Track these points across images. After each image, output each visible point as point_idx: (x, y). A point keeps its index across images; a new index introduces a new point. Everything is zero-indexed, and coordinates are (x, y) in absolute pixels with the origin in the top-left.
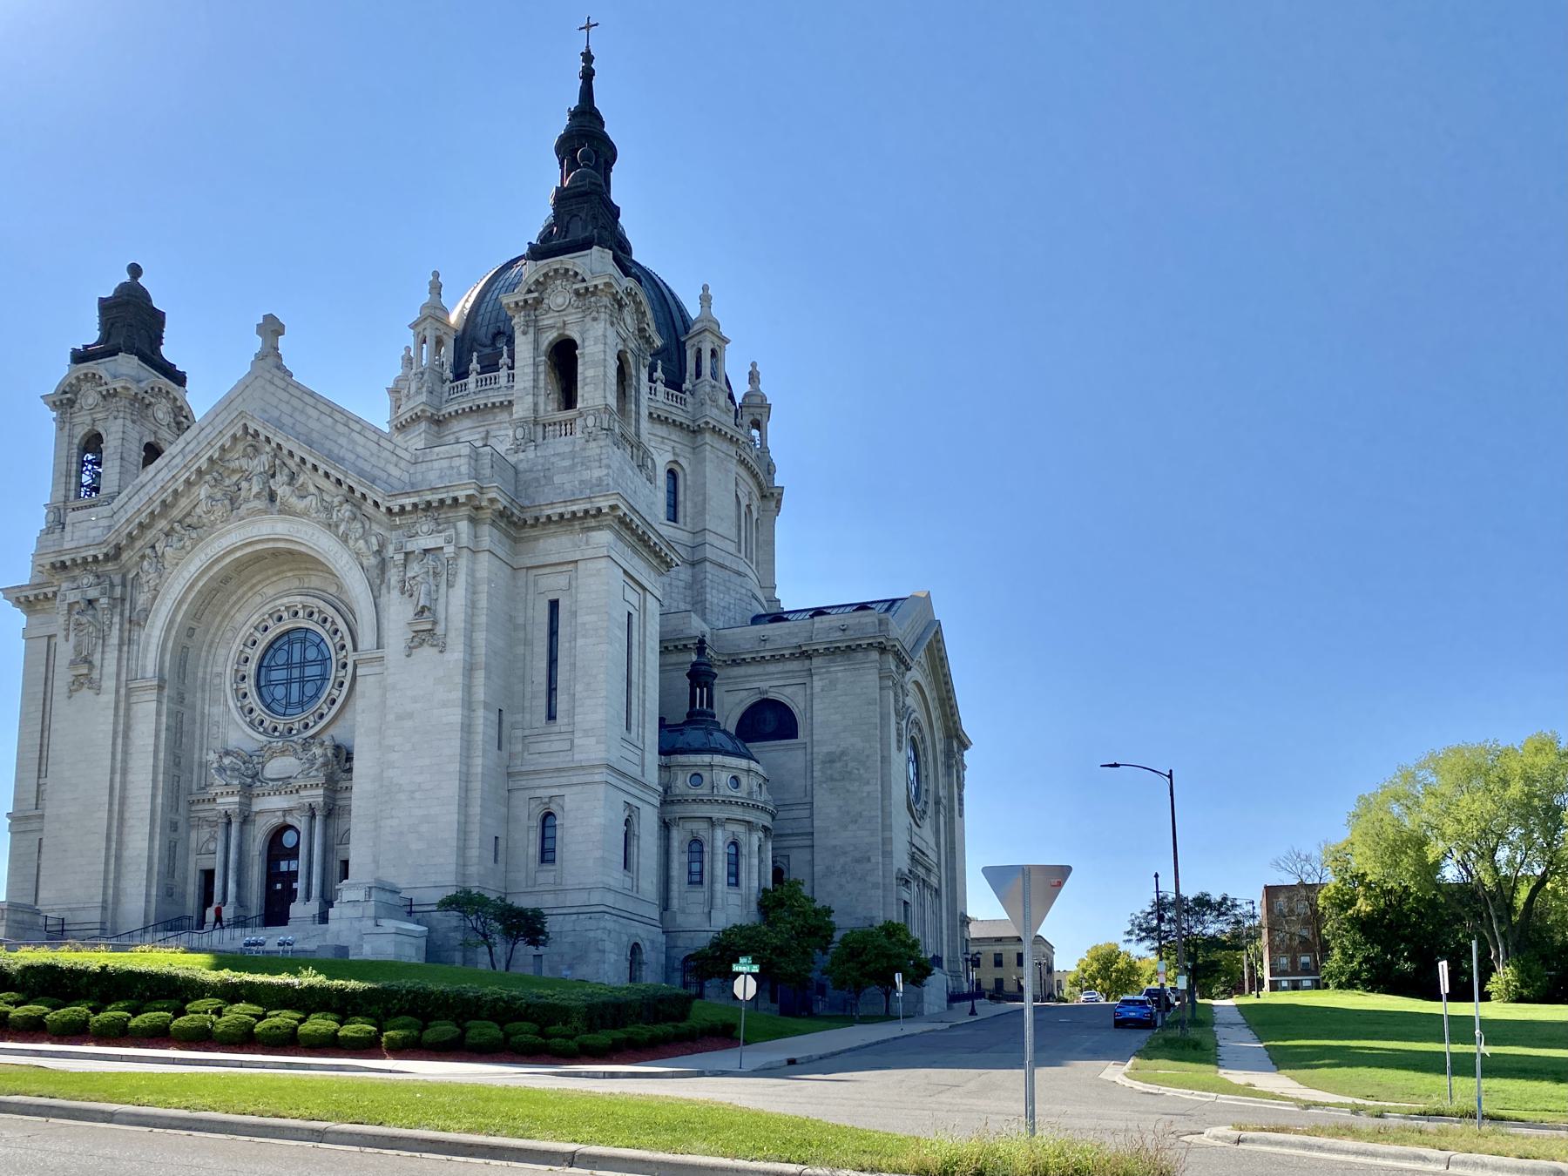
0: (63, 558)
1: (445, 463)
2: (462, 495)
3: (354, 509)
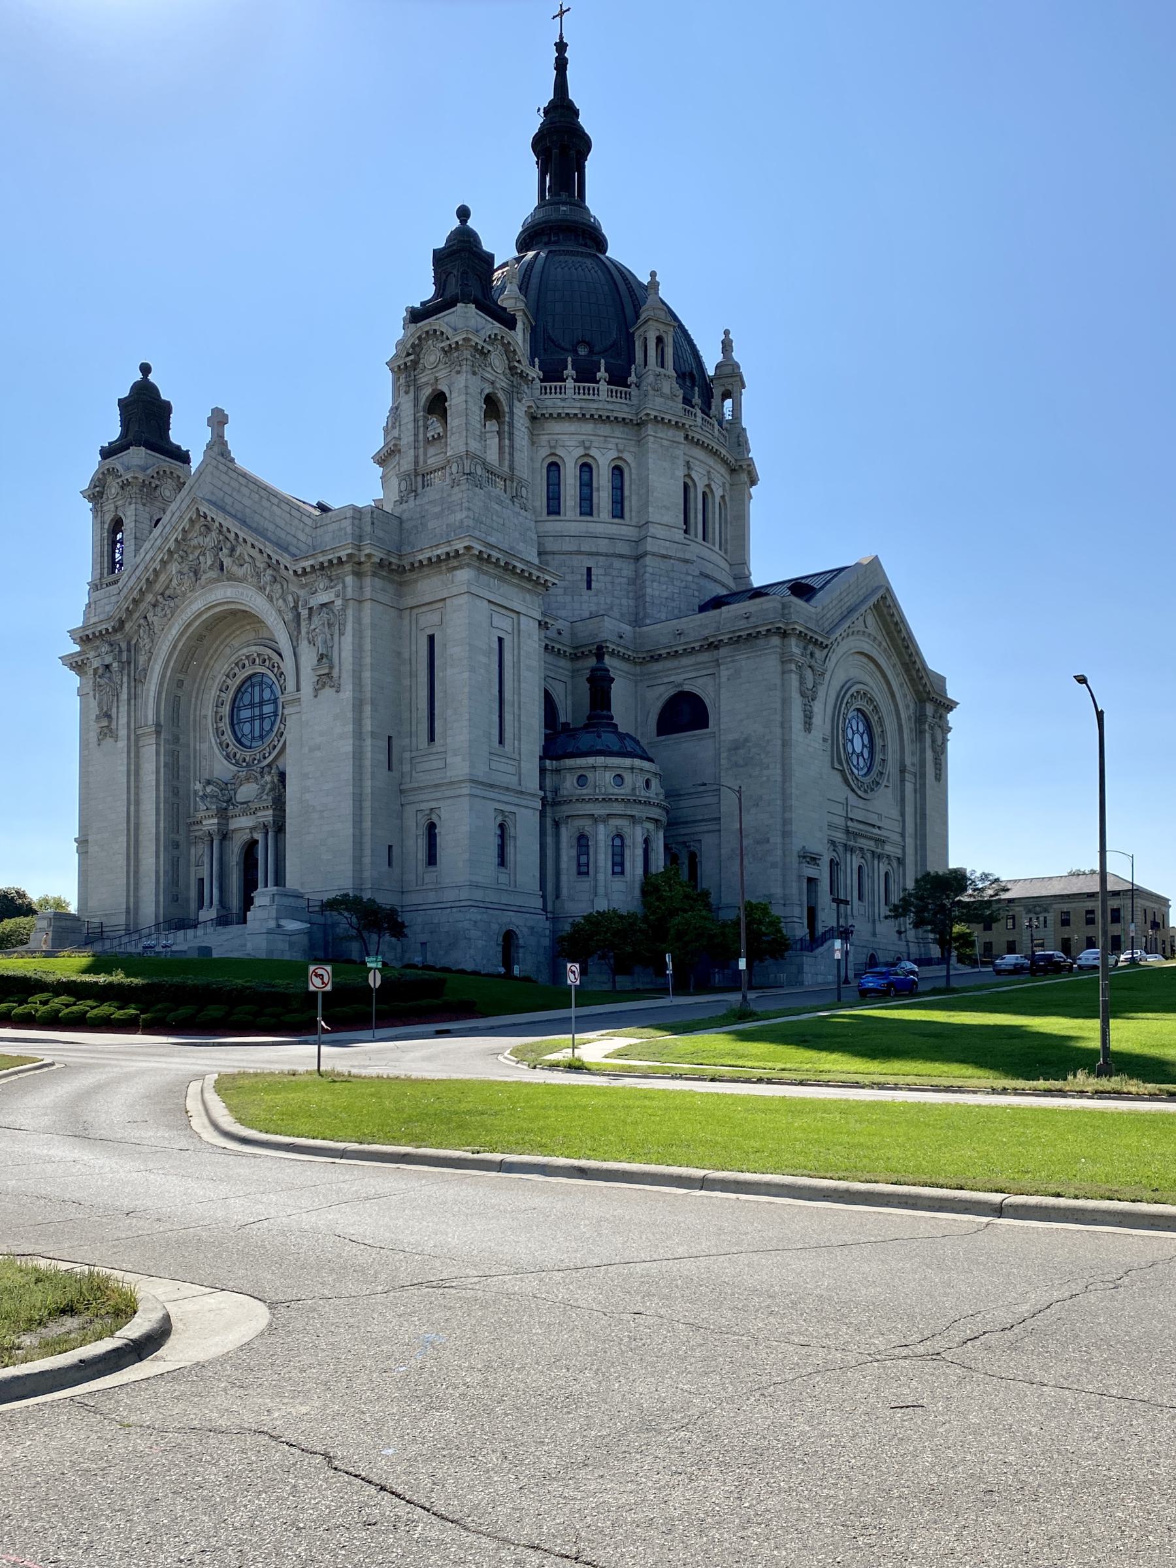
0: (87, 633)
1: (335, 526)
2: (343, 554)
3: (274, 573)
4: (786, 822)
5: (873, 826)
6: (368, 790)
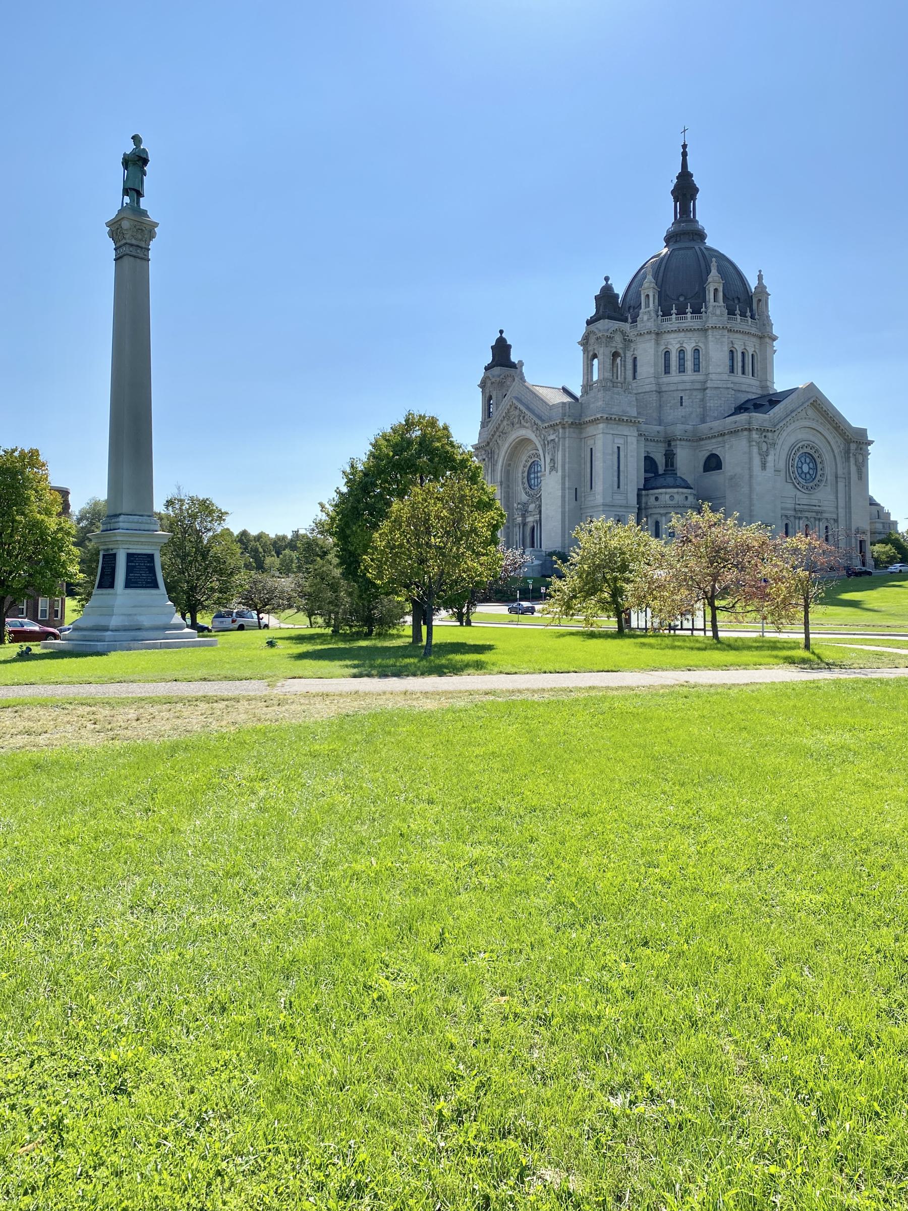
4: (751, 511)
5: (815, 506)
6: (567, 510)
